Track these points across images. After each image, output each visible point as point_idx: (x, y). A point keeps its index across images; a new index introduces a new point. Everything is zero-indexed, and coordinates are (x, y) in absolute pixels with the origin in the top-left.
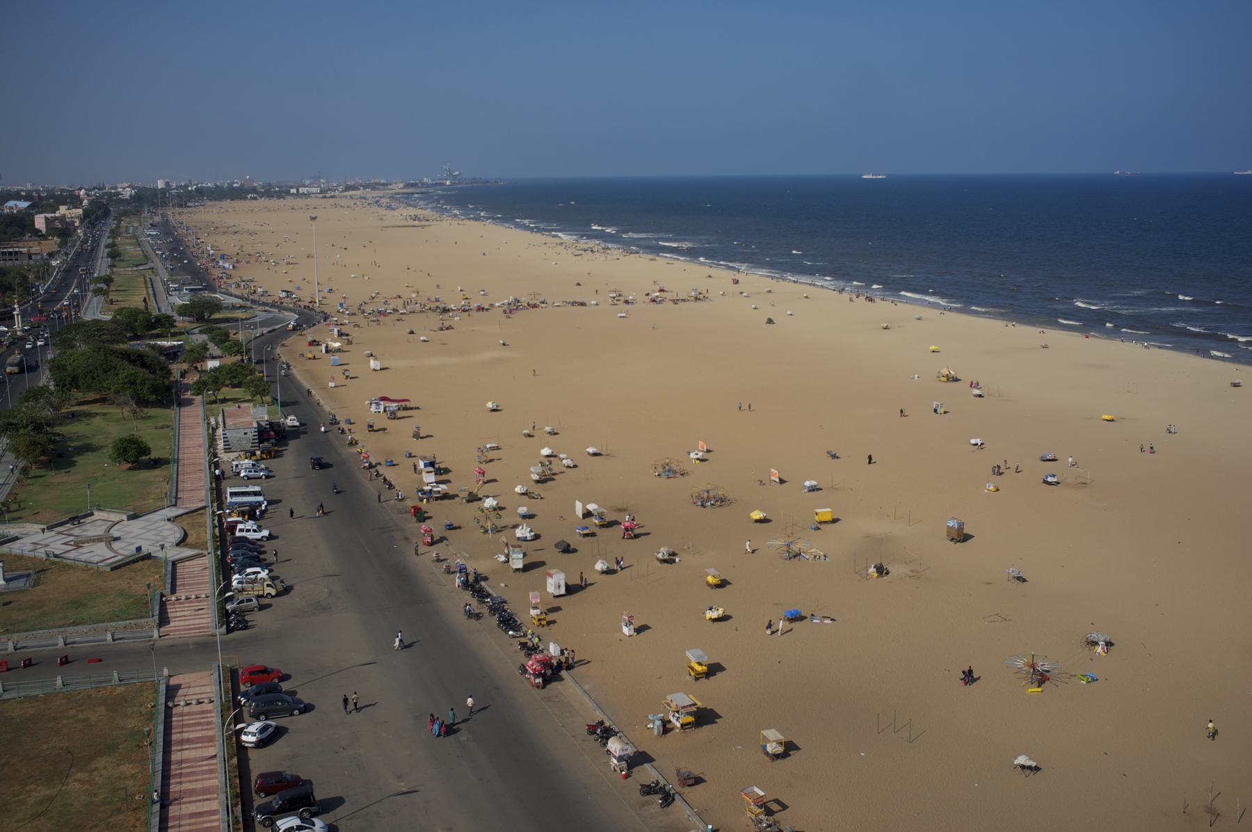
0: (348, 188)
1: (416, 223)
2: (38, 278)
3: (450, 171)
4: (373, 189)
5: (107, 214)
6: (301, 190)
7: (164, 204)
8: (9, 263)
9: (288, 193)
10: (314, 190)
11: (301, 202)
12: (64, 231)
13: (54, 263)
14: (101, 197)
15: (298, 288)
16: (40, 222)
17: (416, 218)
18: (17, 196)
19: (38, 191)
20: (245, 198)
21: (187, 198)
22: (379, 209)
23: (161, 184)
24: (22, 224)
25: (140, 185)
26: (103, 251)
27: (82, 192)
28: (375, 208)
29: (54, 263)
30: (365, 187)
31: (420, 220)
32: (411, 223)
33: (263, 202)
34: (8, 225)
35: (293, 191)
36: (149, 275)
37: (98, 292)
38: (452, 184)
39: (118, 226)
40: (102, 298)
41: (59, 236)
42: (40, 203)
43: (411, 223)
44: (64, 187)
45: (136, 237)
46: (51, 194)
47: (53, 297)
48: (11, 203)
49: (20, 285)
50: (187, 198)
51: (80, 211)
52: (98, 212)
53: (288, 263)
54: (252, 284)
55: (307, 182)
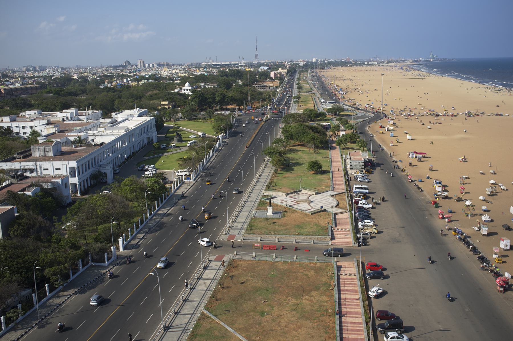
0: (388, 62)
1: (419, 77)
2: (274, 96)
3: (433, 55)
4: (399, 62)
5: (295, 72)
6: (370, 63)
7: (316, 68)
8: (262, 90)
9: (364, 64)
10: (375, 63)
11: (369, 68)
12: (281, 78)
13: (278, 90)
14: (293, 65)
15: (373, 103)
16: (272, 75)
17: (419, 75)
18: (263, 65)
19: (270, 63)
20: (347, 66)
21: (324, 66)
22: (402, 71)
23: (314, 60)
24: (266, 75)
25: (306, 60)
26: (295, 86)
27: (286, 63)
28: (401, 71)
29: (278, 90)
30: (396, 62)
31: (421, 76)
32: (417, 77)
34: (262, 76)
35: (366, 63)
36: (313, 95)
37: (296, 102)
38: (433, 61)
39: (300, 76)
40: (297, 104)
41: (279, 80)
43: (417, 77)
44: (279, 61)
45: (306, 81)
46: (275, 64)
47: (279, 104)
48: (262, 67)
49: (268, 98)
50: (324, 66)
51: (286, 71)
52: (292, 71)
53: (367, 93)
54: (354, 101)
55: (372, 59)
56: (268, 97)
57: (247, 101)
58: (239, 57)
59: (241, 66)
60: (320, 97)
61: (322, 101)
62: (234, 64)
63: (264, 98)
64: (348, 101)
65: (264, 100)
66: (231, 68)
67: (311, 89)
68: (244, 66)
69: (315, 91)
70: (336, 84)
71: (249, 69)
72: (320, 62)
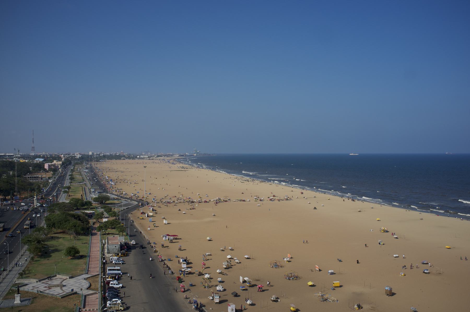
0: (158, 156)
1: (183, 169)
2: (44, 186)
5: (70, 163)
7: (91, 160)
8: (34, 181)
9: (136, 157)
10: (146, 157)
11: (141, 161)
12: (54, 170)
13: (50, 181)
14: (69, 157)
15: (138, 193)
16: (46, 166)
17: (183, 167)
18: (39, 157)
19: (47, 155)
20: (121, 159)
21: (100, 158)
23: (90, 153)
24: (40, 167)
25: (83, 153)
26: (68, 177)
27: (62, 156)
28: (168, 164)
29: (50, 181)
30: (164, 156)
33: (127, 160)
34: (35, 167)
35: (138, 157)
36: (84, 186)
37: (65, 192)
39: (74, 168)
40: (66, 194)
42: (47, 159)
46: (51, 156)
47: (48, 193)
48: (37, 159)
49: (37, 189)
50: (100, 158)
51: (61, 162)
52: (67, 163)
53: (135, 183)
54: (121, 191)
55: (144, 154)
56: (36, 187)
57: (15, 192)
58: (15, 149)
59: (16, 157)
60: (90, 187)
61: (92, 190)
62: (9, 156)
63: (33, 189)
64: (116, 191)
65: (33, 190)
66: (4, 160)
67: (83, 179)
68: (19, 158)
69: (88, 183)
70: (107, 175)
71: (24, 161)
72: (96, 155)
